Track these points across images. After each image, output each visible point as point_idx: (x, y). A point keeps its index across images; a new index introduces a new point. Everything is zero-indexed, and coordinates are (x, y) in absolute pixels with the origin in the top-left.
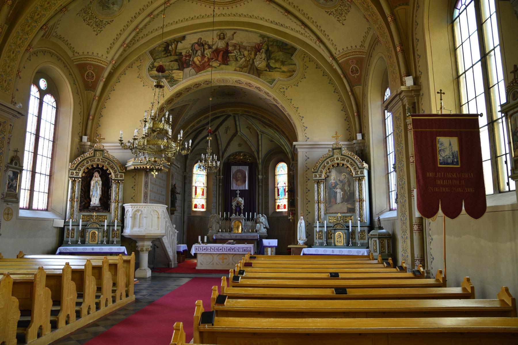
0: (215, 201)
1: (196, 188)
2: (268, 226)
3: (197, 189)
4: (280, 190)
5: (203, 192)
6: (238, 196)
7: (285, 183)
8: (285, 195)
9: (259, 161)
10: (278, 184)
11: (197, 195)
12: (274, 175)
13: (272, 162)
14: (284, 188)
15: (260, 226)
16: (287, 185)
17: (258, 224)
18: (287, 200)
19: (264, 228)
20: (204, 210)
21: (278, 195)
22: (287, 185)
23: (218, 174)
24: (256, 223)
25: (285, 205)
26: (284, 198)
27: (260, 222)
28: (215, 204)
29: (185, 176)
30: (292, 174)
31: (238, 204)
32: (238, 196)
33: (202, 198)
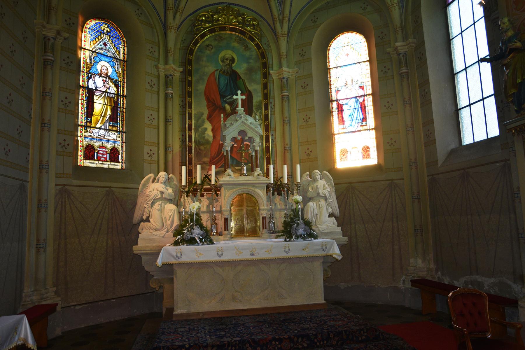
0: (155, 140)
1: (91, 93)
2: (337, 212)
3: (95, 98)
4: (345, 107)
5: (115, 110)
6: (240, 109)
7: (362, 87)
8: (364, 119)
9: (282, 27)
10: (337, 91)
11: (94, 118)
12: (325, 70)
13: (318, 31)
14: (361, 100)
15: (320, 207)
16: (369, 90)
17: (311, 204)
18: (373, 132)
19: (330, 216)
20: (117, 166)
21: (342, 121)
22: (370, 92)
23: (162, 61)
24: (306, 200)
25: (366, 150)
26: (361, 128)
27: (318, 194)
28: (155, 149)
29: (45, 37)
30: (401, 51)
31: (242, 133)
32: (240, 109)
33: (111, 128)
